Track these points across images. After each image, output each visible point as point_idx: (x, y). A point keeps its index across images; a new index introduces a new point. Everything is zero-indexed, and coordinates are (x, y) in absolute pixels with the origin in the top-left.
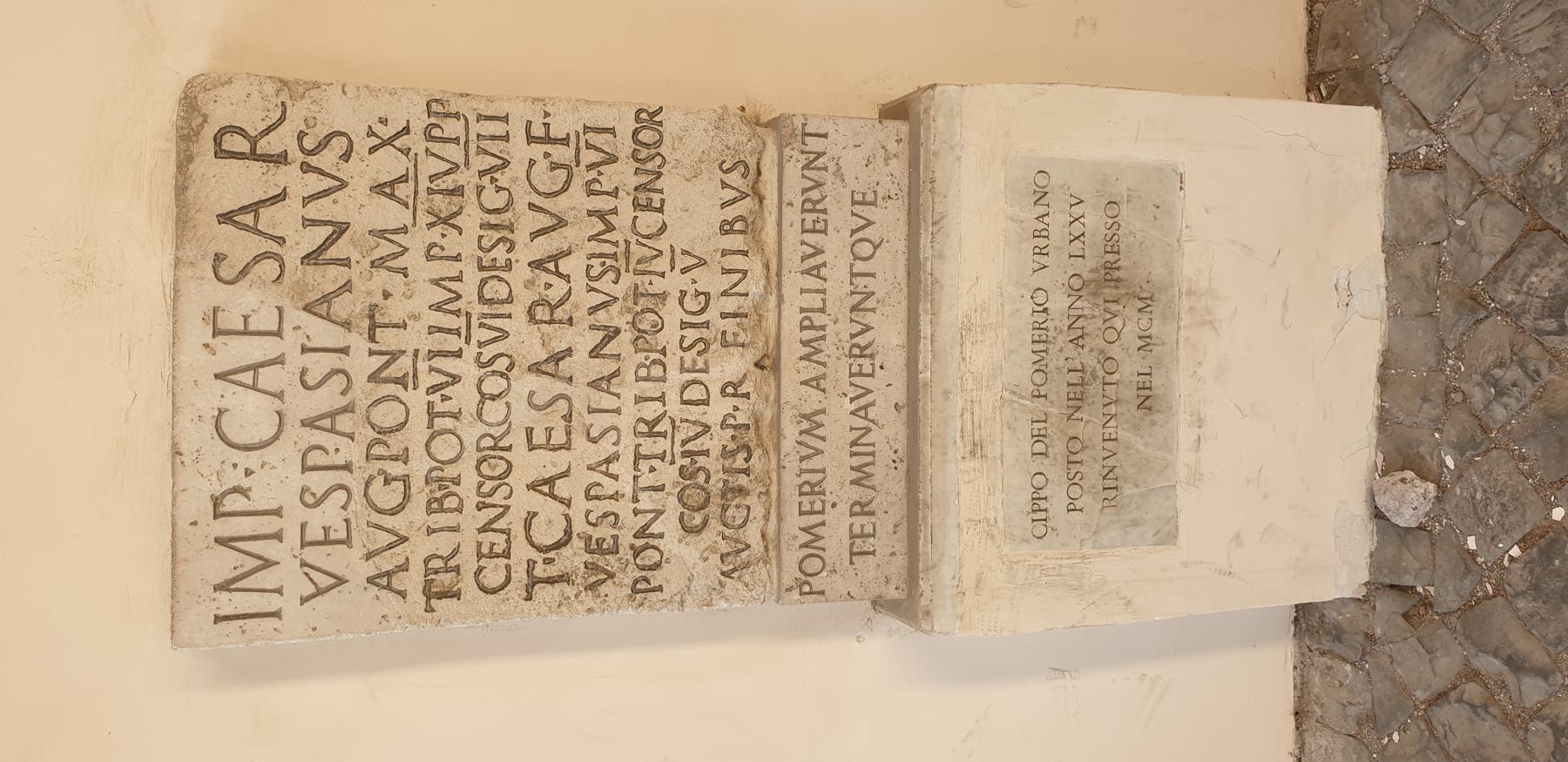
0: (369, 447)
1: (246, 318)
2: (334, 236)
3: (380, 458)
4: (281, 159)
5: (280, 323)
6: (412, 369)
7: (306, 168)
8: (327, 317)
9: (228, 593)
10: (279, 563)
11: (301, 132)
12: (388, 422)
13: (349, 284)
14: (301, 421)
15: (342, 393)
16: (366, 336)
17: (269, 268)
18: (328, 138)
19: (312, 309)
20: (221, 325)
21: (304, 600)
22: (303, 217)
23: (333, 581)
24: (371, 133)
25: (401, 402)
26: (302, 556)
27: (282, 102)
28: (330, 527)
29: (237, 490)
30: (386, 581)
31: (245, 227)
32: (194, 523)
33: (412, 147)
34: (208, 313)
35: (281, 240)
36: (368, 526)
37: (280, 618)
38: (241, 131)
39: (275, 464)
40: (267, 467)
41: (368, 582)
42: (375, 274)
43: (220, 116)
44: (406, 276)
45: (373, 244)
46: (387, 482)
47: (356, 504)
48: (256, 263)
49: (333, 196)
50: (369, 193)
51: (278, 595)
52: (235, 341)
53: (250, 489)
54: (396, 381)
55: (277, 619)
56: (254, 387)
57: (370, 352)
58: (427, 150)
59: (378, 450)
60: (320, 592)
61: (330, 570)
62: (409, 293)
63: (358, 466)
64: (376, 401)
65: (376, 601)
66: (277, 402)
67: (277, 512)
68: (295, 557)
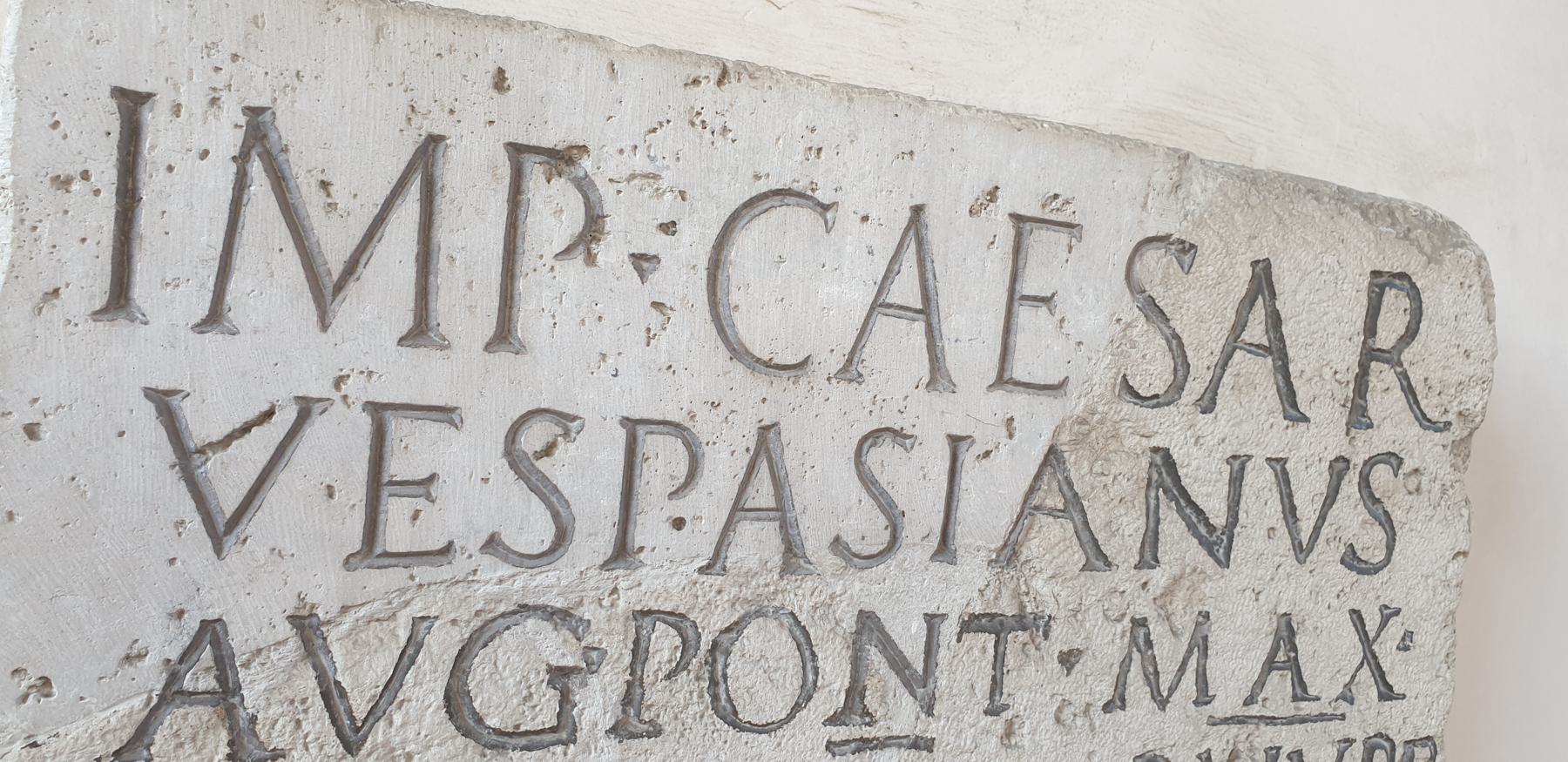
0: (676, 619)
1: (1046, 300)
2: (1203, 530)
3: (639, 653)
4: (1358, 417)
5: (1027, 385)
6: (882, 734)
7: (1340, 467)
8: (1029, 508)
9: (235, 151)
10: (324, 326)
11: (1401, 461)
12: (740, 673)
13: (1100, 564)
14: (775, 425)
15: (837, 539)
16: (978, 610)
17: (1154, 374)
18: (1383, 519)
19: (1049, 470)
20: (1042, 242)
21: (164, 403)
22: (1249, 457)
23: (228, 499)
24: (1388, 614)
25: (797, 708)
26: (339, 406)
27: (1450, 423)
28: (429, 497)
29: (593, 227)
30: (201, 686)
31: (1240, 326)
32: (500, 81)
33: (1355, 707)
34: (1070, 209)
35: (1208, 404)
36: (416, 621)
37: (98, 315)
38: (1411, 333)
39: (662, 342)
40: (655, 318)
41: (205, 624)
42: (1119, 627)
43: (1440, 294)
44: (1107, 708)
45: (1178, 622)
46: (559, 676)
47: (501, 581)
48: (1167, 340)
49: (1282, 530)
50: (1281, 611)
51: (202, 310)
52: (997, 266)
53: (591, 259)
54: (855, 691)
55: (100, 302)
56: (879, 305)
57: (933, 616)
58: (1349, 741)
59: (664, 644)
60: (186, 458)
61: (273, 496)
62: (1067, 714)
63: (622, 585)
64: (807, 635)
65: (121, 651)
66: (836, 363)
67: (504, 336)
68: (339, 382)
